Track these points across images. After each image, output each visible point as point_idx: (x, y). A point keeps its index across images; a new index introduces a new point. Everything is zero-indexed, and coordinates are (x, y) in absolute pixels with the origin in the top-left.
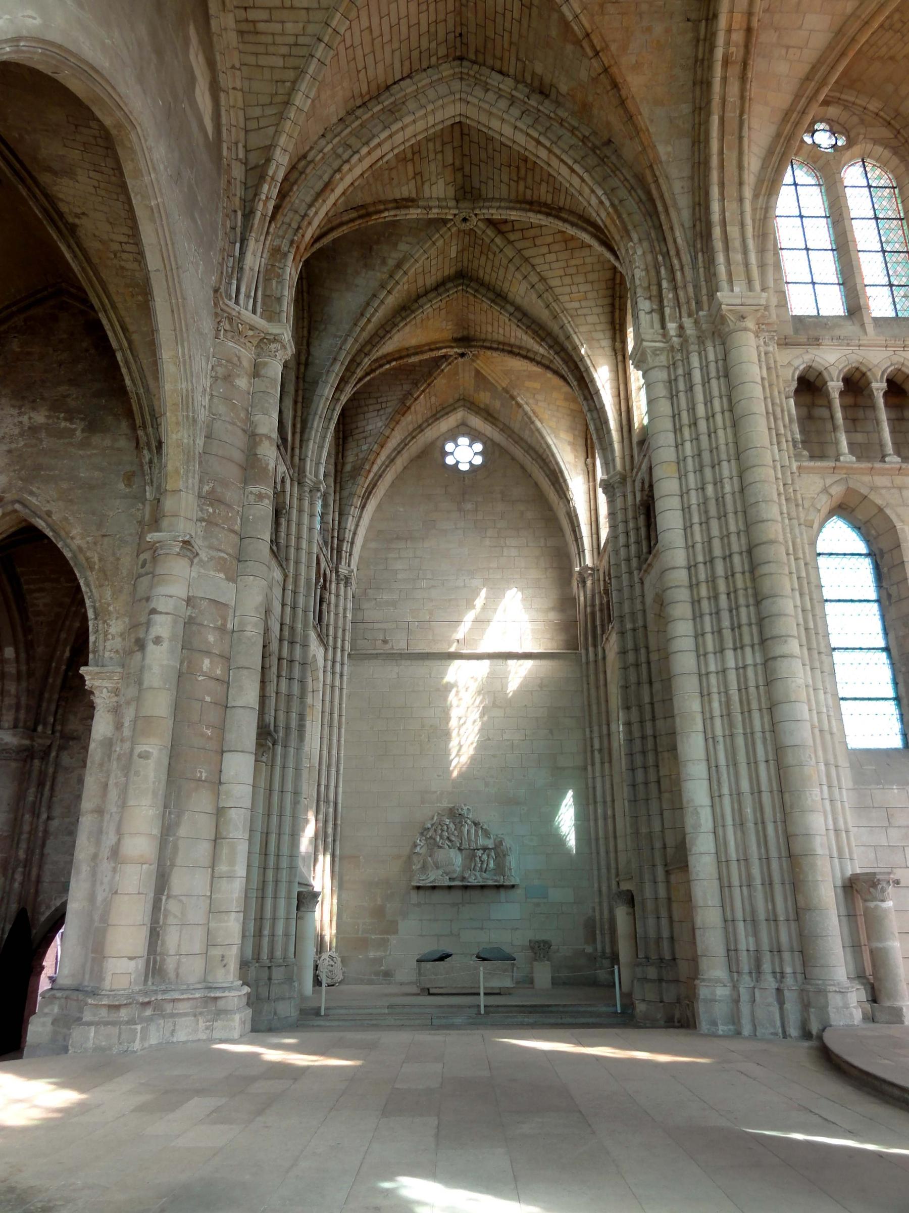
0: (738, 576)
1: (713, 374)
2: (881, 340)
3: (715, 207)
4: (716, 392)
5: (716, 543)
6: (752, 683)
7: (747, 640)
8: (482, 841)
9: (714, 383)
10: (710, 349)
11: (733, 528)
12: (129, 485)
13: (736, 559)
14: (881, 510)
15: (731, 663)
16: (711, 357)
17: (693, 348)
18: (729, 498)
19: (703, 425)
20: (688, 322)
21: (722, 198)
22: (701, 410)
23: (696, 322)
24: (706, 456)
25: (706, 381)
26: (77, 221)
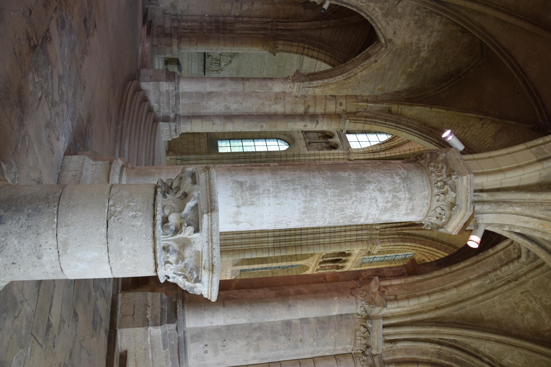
0: (294, 242)
1: (358, 237)
2: (358, 258)
3: (409, 244)
4: (352, 238)
5: (306, 236)
6: (263, 245)
7: (275, 244)
8: (223, 64)
9: (355, 237)
10: (366, 237)
11: (309, 241)
12: (379, 89)
13: (300, 242)
14: (308, 258)
15: (270, 239)
16: (364, 237)
17: (369, 232)
18: (318, 241)
19: (343, 233)
20: (378, 232)
21: (410, 246)
22: (348, 233)
23: (376, 234)
24: (333, 234)
25: (357, 235)
26: (482, 122)
